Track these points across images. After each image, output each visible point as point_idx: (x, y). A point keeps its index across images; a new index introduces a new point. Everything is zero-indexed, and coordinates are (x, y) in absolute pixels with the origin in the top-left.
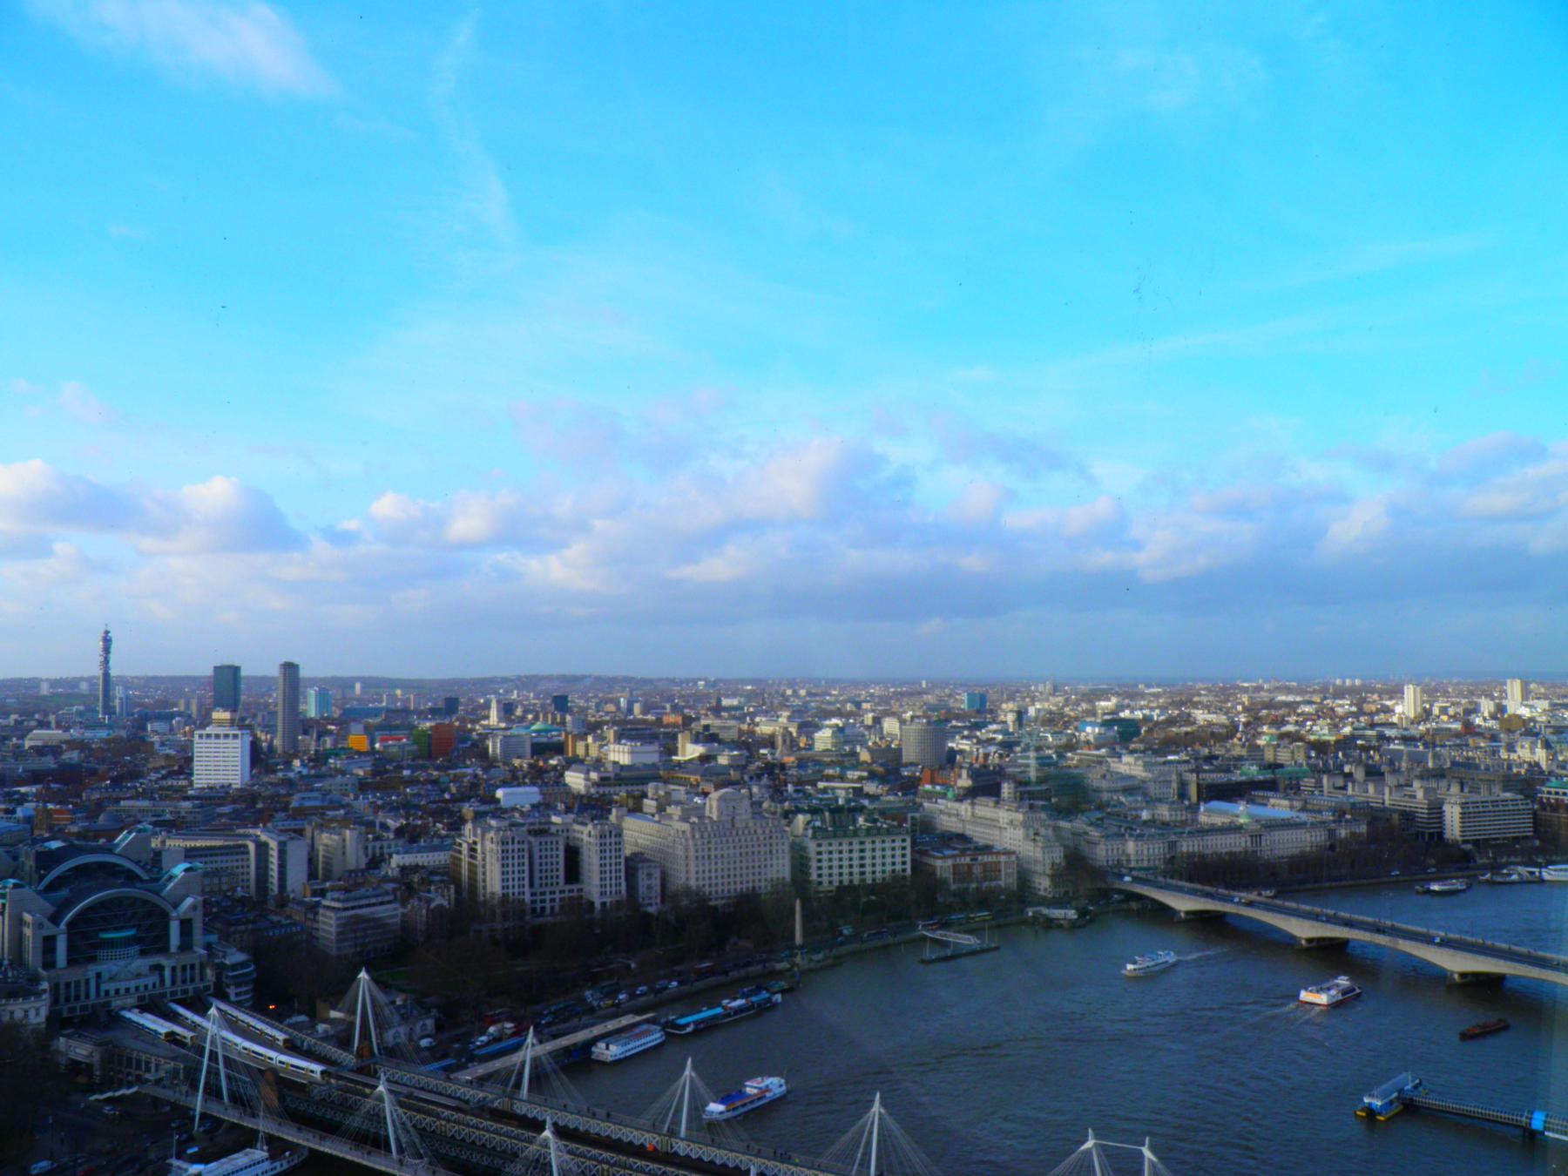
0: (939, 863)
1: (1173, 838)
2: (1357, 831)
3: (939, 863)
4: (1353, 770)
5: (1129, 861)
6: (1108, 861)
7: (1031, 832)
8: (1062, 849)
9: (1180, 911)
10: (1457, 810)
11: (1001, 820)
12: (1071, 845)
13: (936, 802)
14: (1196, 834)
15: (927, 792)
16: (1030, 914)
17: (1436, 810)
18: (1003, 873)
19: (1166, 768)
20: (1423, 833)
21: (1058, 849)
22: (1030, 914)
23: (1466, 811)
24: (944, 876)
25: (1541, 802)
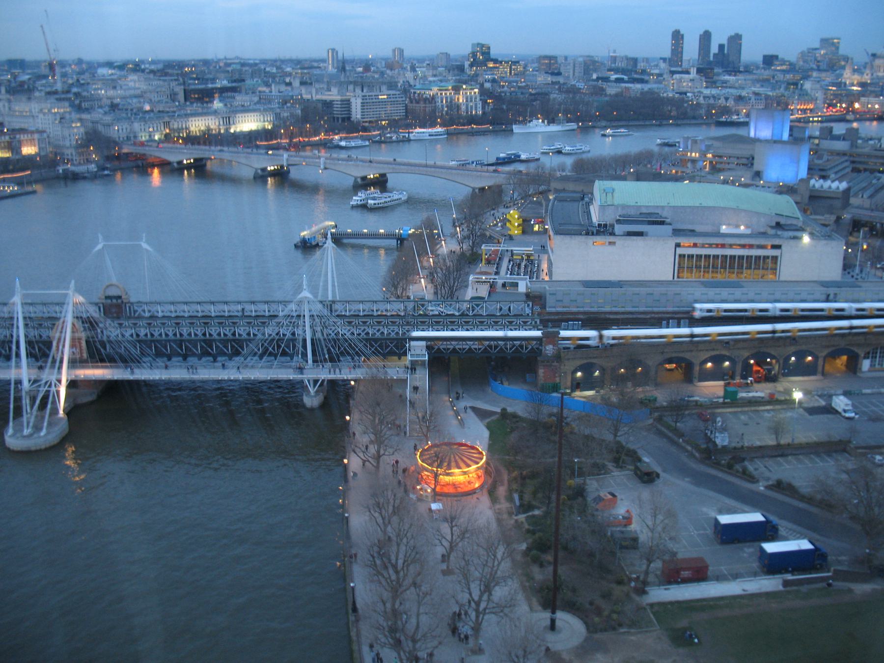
1: (167, 119)
4: (292, 80)
6: (119, 138)
10: (359, 101)
16: (61, 171)
17: (347, 104)
20: (338, 118)
23: (365, 101)
25: (410, 98)
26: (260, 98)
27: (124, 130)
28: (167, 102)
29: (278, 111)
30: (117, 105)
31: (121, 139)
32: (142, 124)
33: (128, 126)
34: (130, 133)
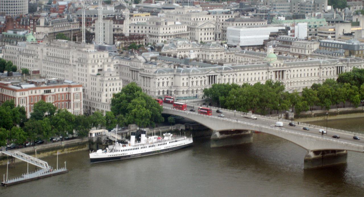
0: (18, 95)
1: (212, 73)
2: (360, 68)
3: (18, 95)
5: (176, 92)
7: (96, 69)
8: (121, 82)
9: (215, 131)
11: (71, 59)
12: (131, 80)
13: (16, 45)
14: (232, 70)
15: (9, 36)
16: (94, 135)
18: (72, 102)
19: (211, 17)
21: (118, 82)
22: (94, 135)
24: (21, 106)
26: (320, 46)
27: (165, 84)
28: (214, 45)
29: (340, 64)
30: (160, 48)
31: (161, 94)
32: (185, 78)
33: (169, 80)
34: (171, 87)
